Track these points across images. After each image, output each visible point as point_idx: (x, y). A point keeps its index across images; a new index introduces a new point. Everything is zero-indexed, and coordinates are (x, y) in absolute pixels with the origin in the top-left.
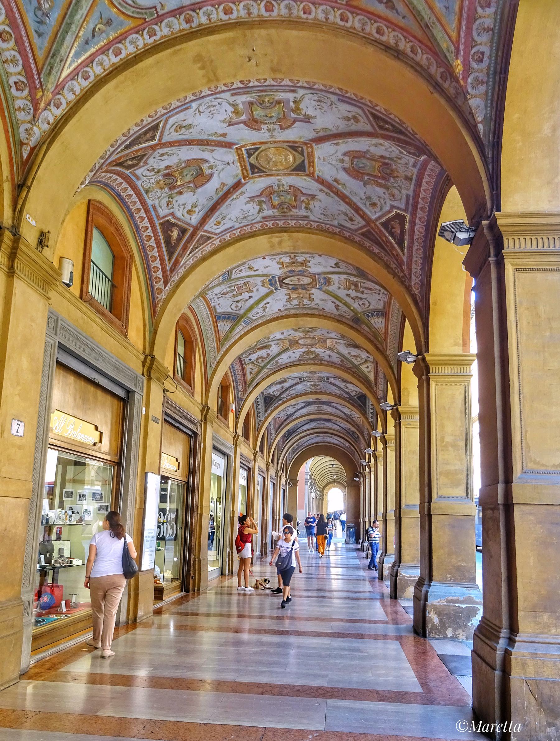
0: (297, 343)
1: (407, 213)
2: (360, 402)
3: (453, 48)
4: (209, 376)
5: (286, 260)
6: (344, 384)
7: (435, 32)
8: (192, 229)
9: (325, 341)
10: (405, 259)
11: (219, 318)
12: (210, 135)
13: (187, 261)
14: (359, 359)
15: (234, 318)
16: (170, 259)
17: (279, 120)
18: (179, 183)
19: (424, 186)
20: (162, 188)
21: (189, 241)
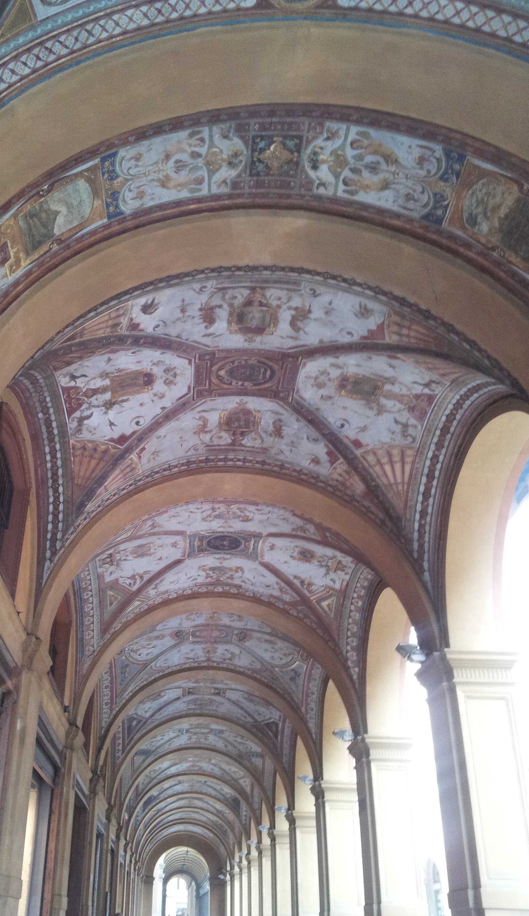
16: (128, 738)
21: (142, 726)
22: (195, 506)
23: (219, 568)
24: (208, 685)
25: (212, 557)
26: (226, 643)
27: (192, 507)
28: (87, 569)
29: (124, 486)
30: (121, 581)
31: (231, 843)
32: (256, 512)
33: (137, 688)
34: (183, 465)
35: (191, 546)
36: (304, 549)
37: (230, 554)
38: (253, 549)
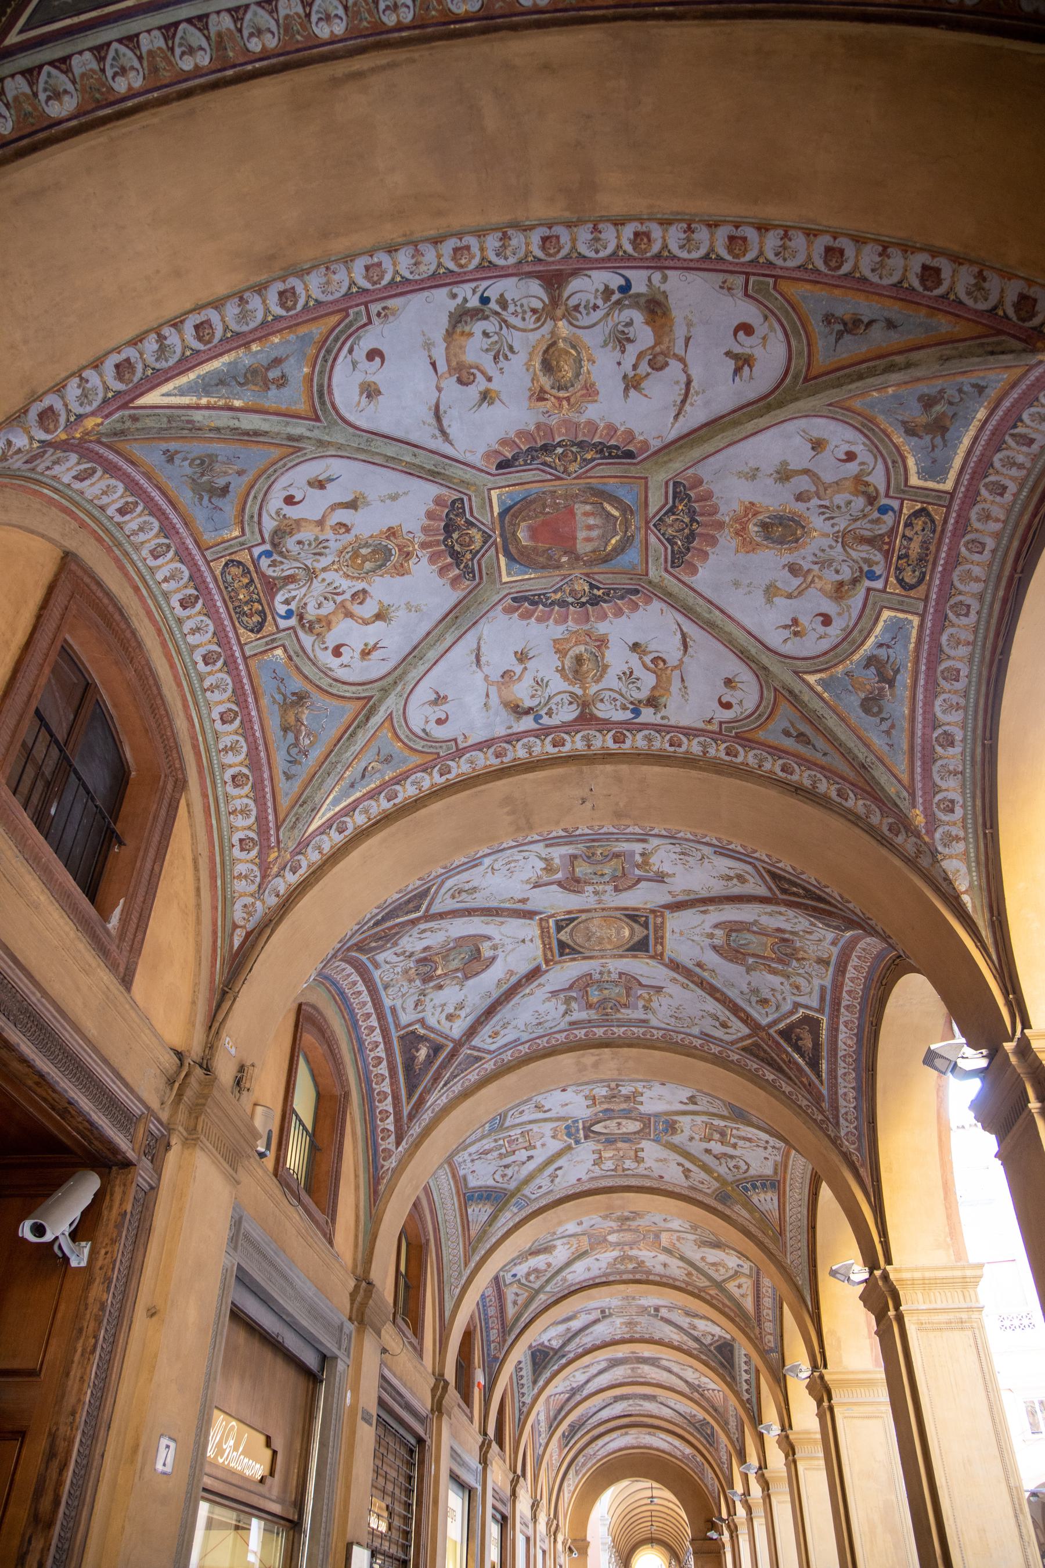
0: (605, 1240)
1: (823, 1014)
2: (721, 1357)
3: (905, 794)
4: (447, 1314)
5: (601, 1091)
6: (688, 1320)
7: (876, 774)
8: (451, 1045)
9: (657, 1236)
10: (825, 1092)
11: (471, 1198)
12: (503, 902)
13: (438, 1098)
14: (722, 1271)
15: (497, 1198)
16: (410, 1096)
17: (614, 878)
18: (439, 972)
19: (851, 972)
20: (410, 981)
21: (443, 1066)
31: (724, 1458)
33: (360, 819)
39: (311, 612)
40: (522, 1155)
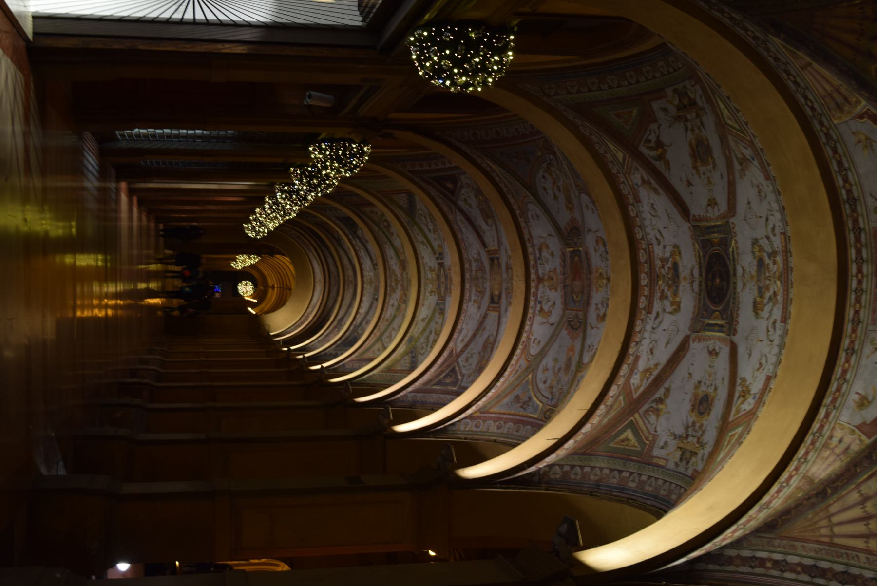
22: (778, 224)
23: (678, 277)
24: (504, 286)
25: (694, 263)
26: (565, 304)
27: (776, 219)
28: (671, 70)
29: (810, 97)
30: (654, 126)
32: (771, 320)
33: (497, 179)
34: (849, 192)
35: (710, 229)
36: (712, 401)
37: (700, 290)
38: (709, 325)
39: (553, 169)
40: (431, 227)
